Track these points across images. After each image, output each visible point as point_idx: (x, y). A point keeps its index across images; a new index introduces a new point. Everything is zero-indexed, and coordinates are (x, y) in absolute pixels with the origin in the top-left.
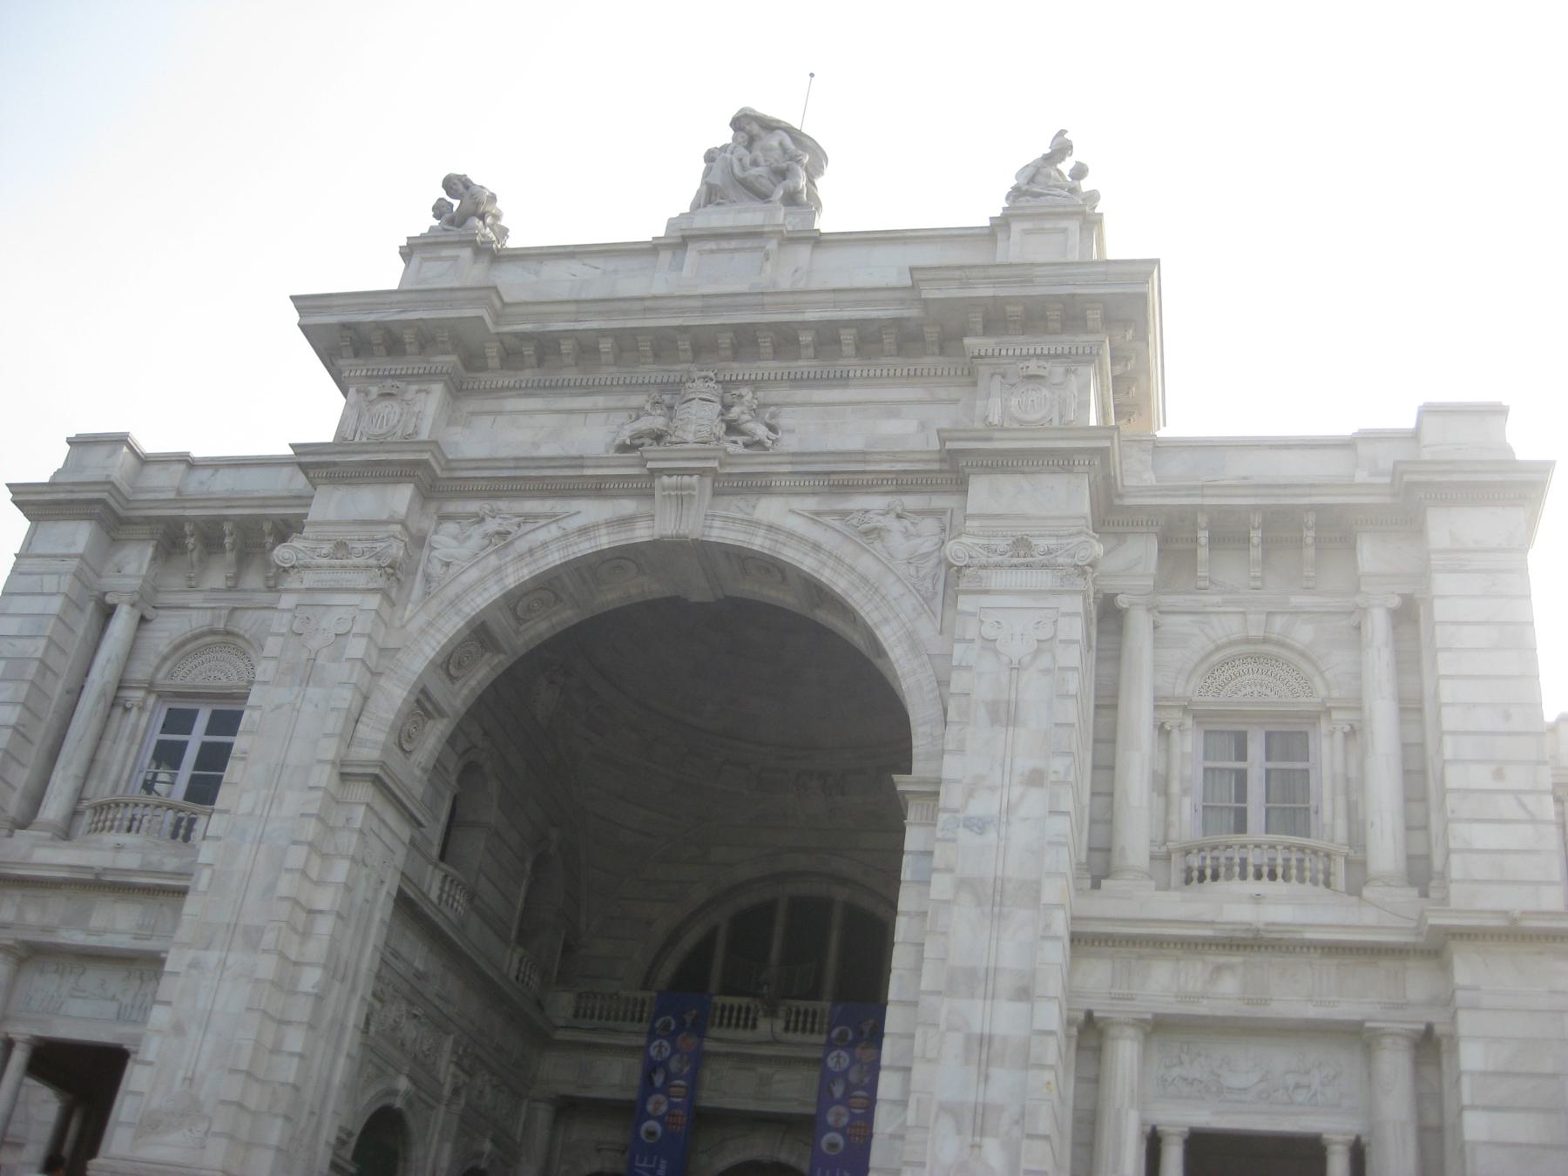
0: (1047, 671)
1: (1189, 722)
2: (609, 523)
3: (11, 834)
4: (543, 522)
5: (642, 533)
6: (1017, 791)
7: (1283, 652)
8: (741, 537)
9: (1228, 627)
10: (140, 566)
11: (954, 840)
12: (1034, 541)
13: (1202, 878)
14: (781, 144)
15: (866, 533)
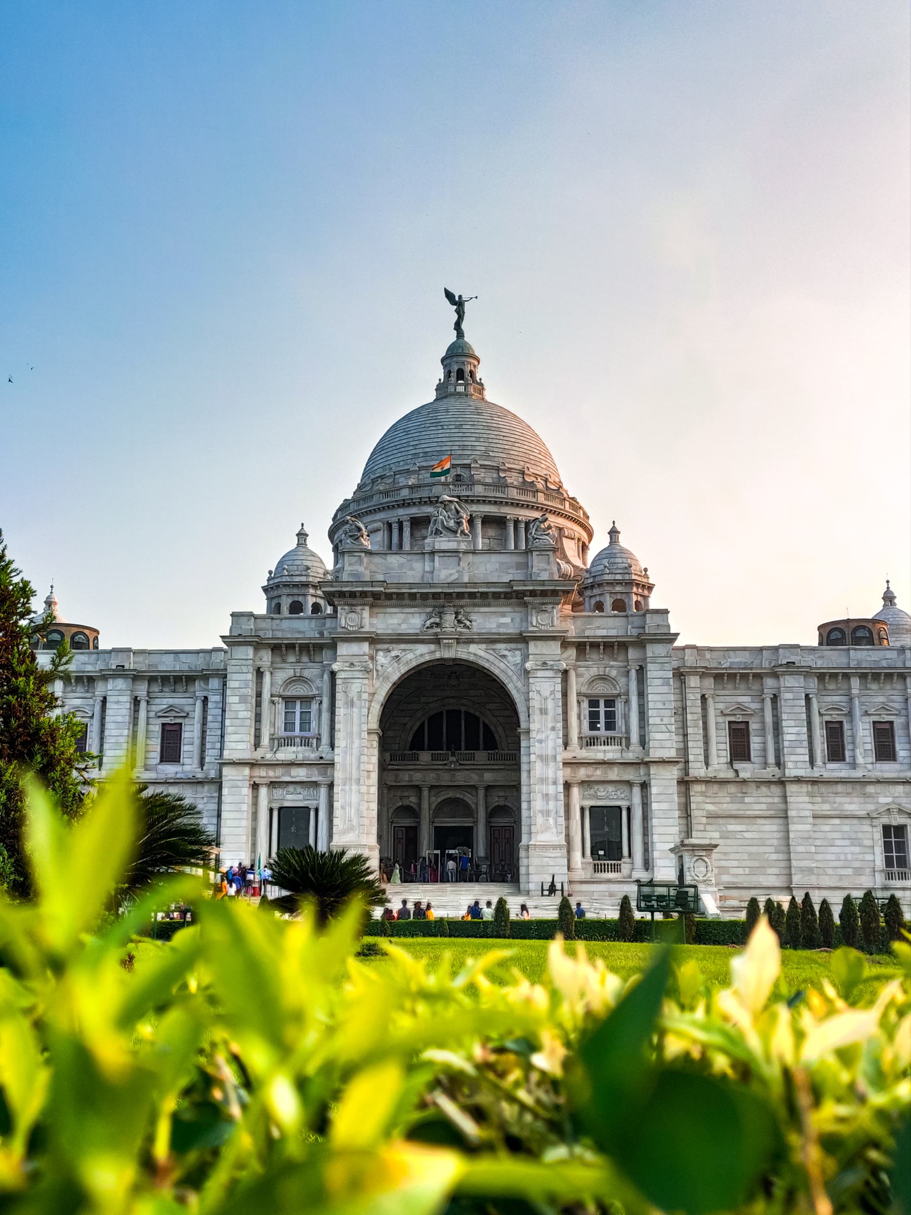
0: (553, 699)
1: (585, 699)
2: (428, 653)
3: (256, 750)
4: (408, 652)
5: (438, 655)
6: (549, 732)
7: (609, 678)
8: (466, 657)
9: (594, 671)
10: (268, 658)
11: (535, 746)
12: (547, 662)
13: (591, 745)
14: (455, 507)
15: (501, 656)
